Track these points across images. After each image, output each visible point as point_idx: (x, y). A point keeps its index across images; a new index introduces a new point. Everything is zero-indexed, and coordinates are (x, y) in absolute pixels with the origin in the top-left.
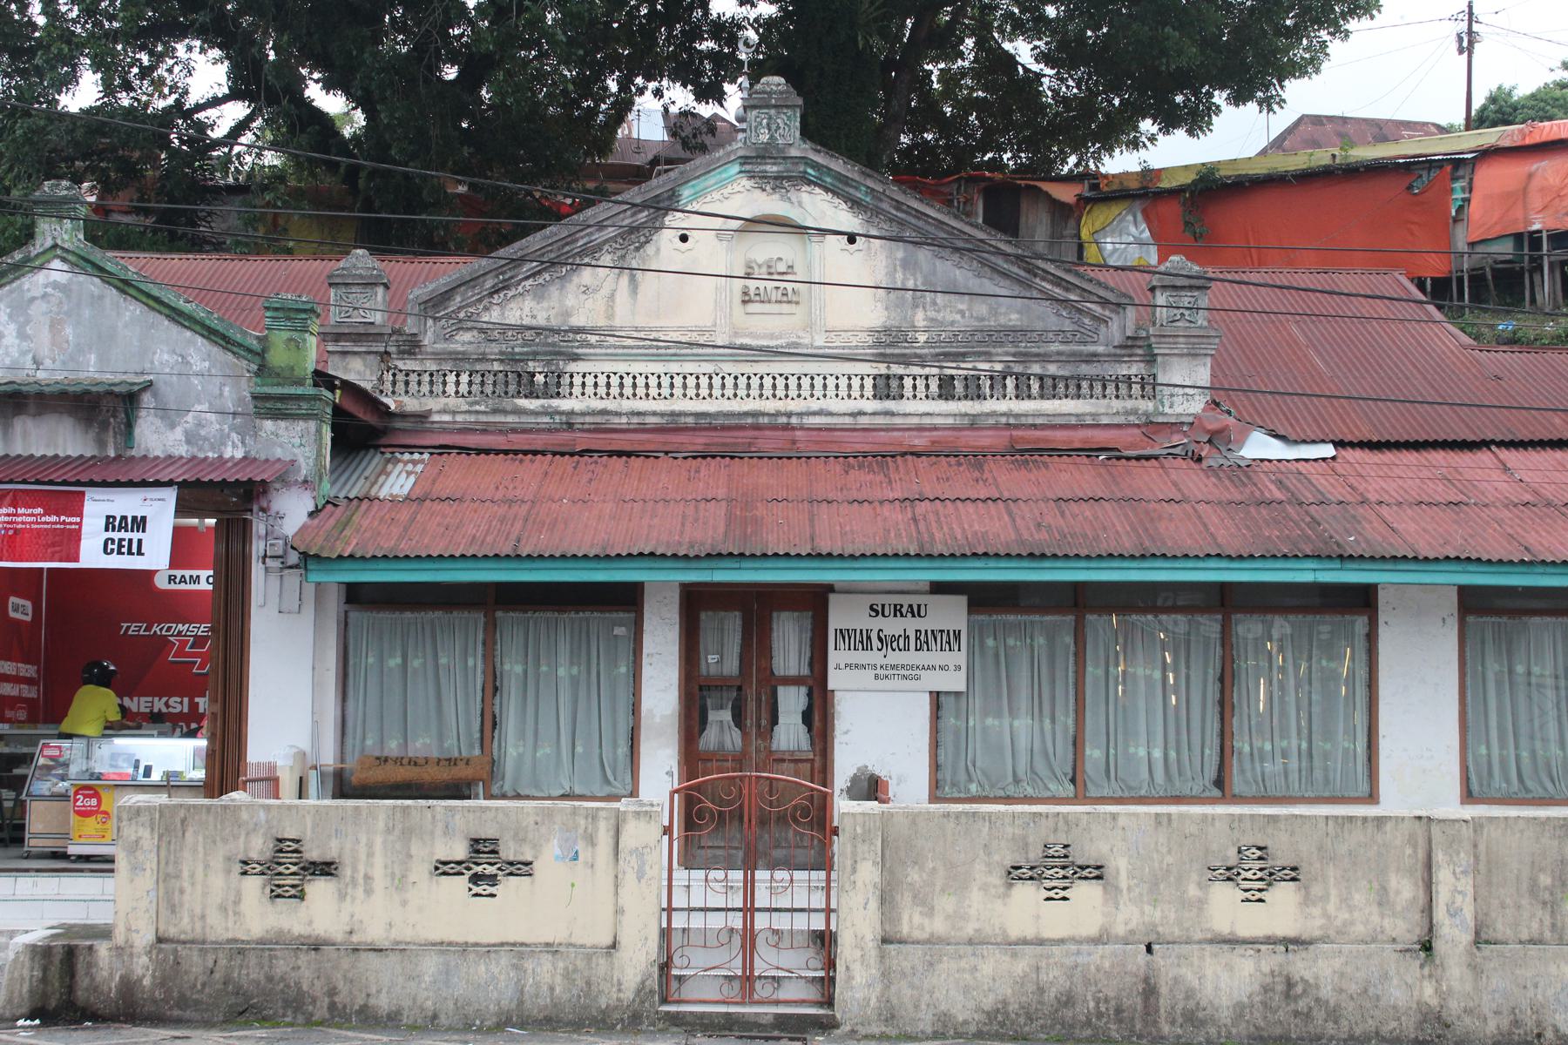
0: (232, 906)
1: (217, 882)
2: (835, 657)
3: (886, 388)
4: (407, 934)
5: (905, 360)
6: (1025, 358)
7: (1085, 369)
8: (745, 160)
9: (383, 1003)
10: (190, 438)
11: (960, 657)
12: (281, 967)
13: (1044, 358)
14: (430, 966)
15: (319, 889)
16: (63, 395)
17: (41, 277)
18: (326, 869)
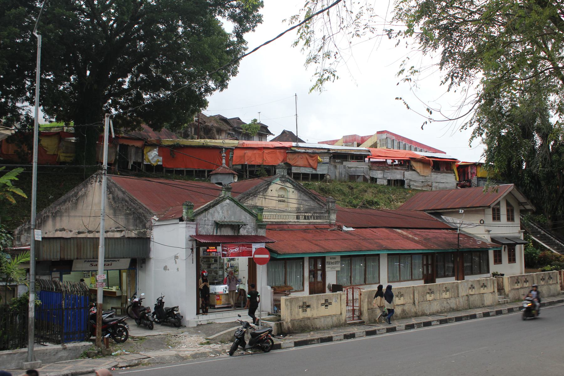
0: (298, 314)
1: (296, 310)
2: (327, 266)
3: (298, 218)
4: (318, 315)
5: (300, 213)
6: (315, 213)
7: (321, 215)
8: (280, 178)
9: (318, 326)
10: (247, 232)
11: (339, 265)
12: (306, 322)
13: (317, 213)
14: (322, 320)
15: (308, 309)
16: (231, 225)
17: (225, 202)
18: (308, 306)
